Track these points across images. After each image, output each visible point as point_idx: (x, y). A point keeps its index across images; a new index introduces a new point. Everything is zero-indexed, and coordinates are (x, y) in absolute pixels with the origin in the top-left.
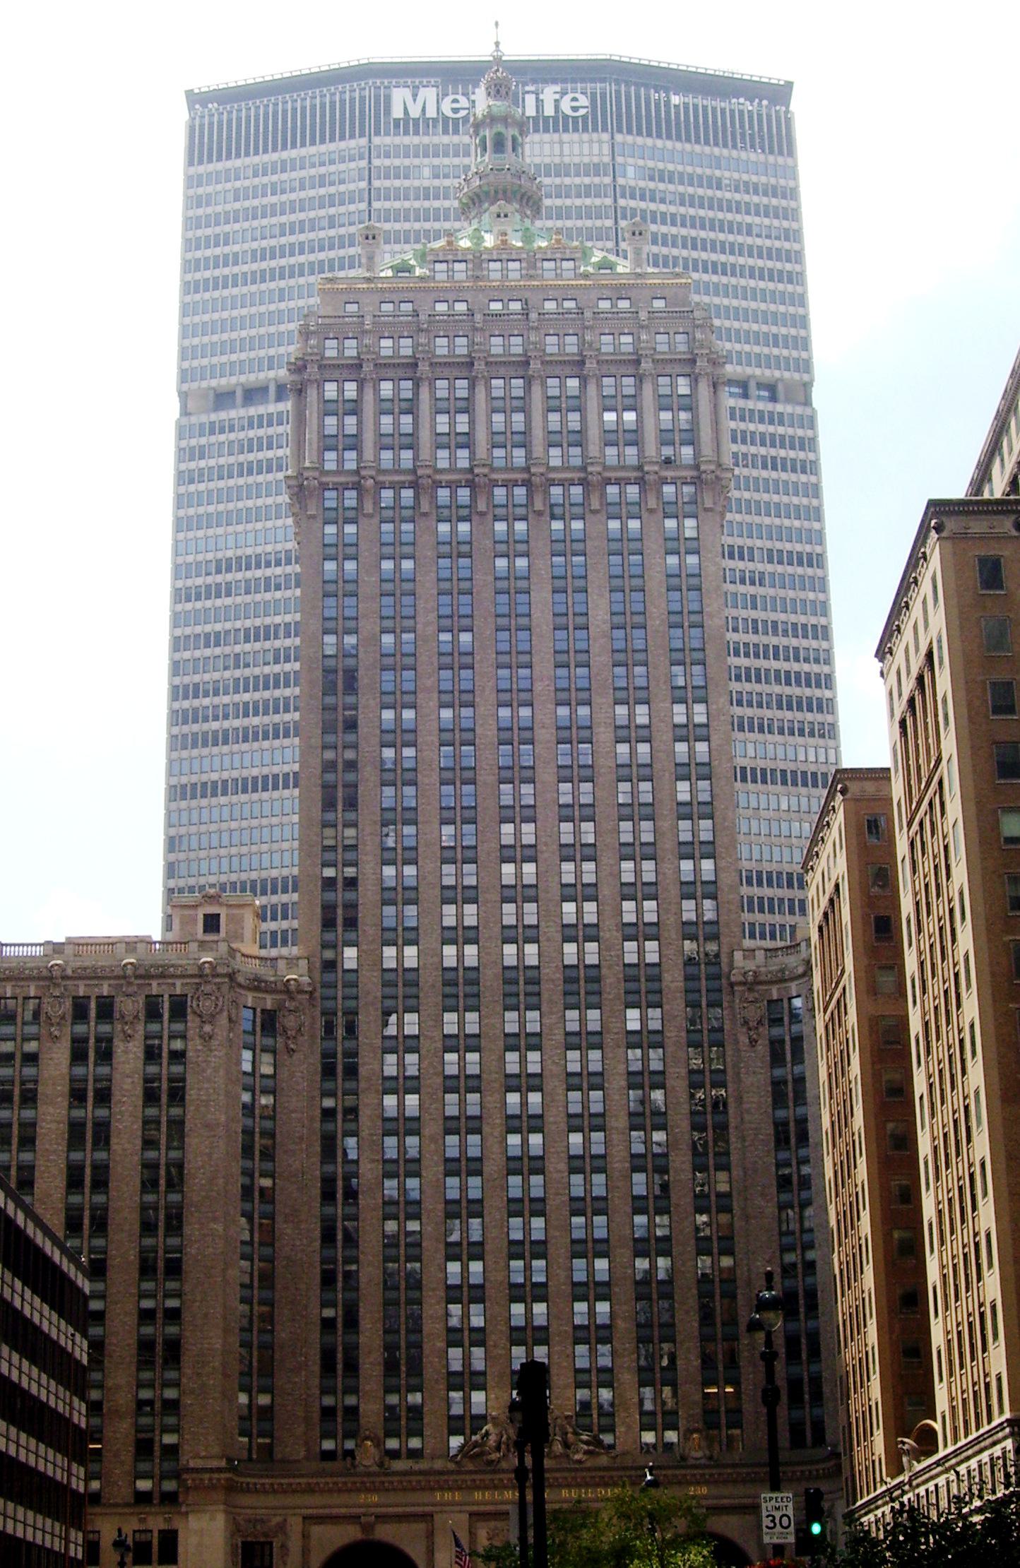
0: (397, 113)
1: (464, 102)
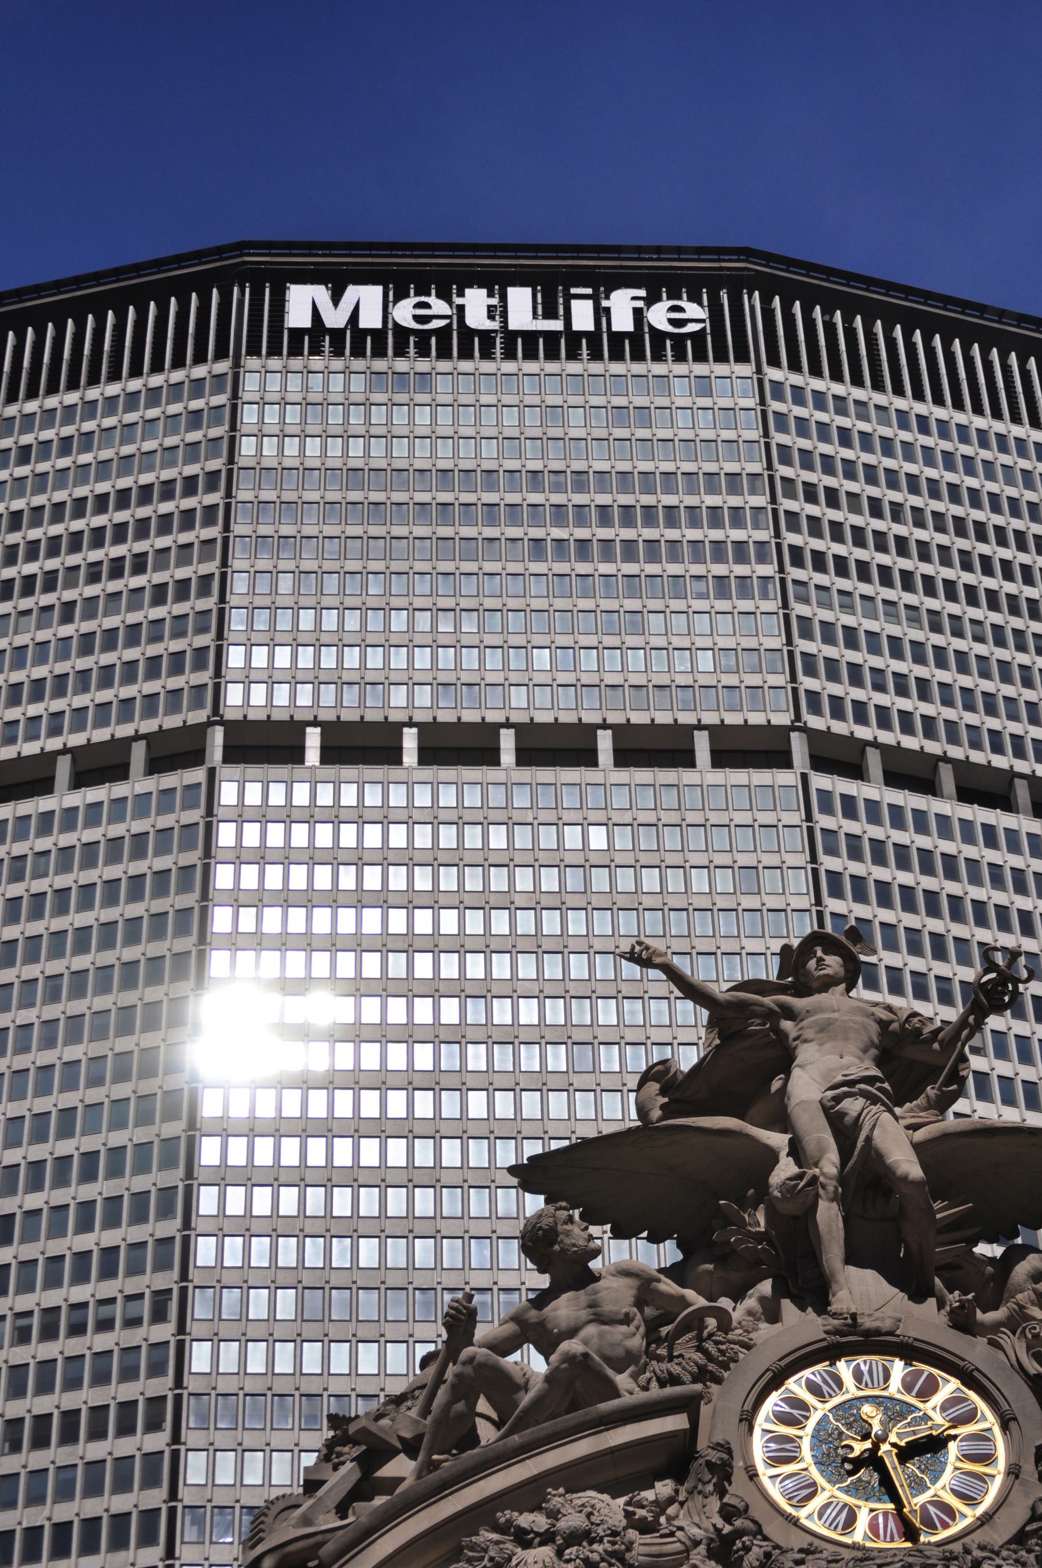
0: (297, 316)
1: (439, 306)
